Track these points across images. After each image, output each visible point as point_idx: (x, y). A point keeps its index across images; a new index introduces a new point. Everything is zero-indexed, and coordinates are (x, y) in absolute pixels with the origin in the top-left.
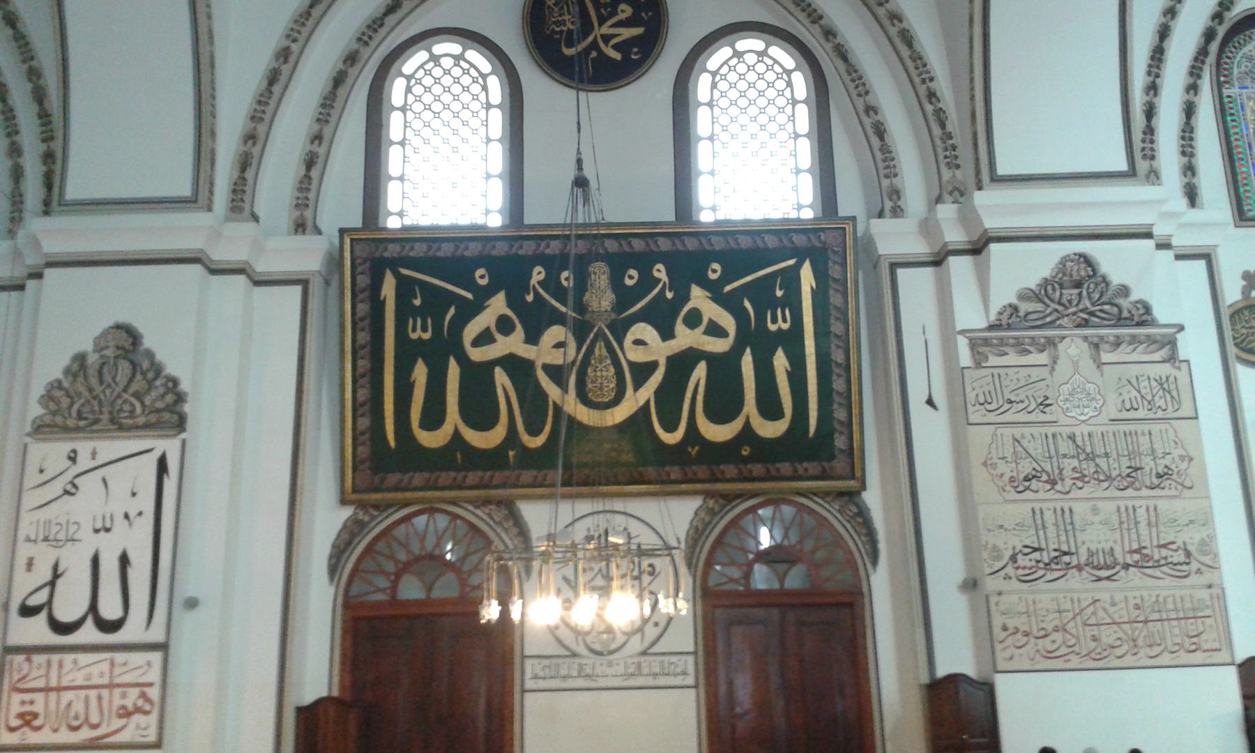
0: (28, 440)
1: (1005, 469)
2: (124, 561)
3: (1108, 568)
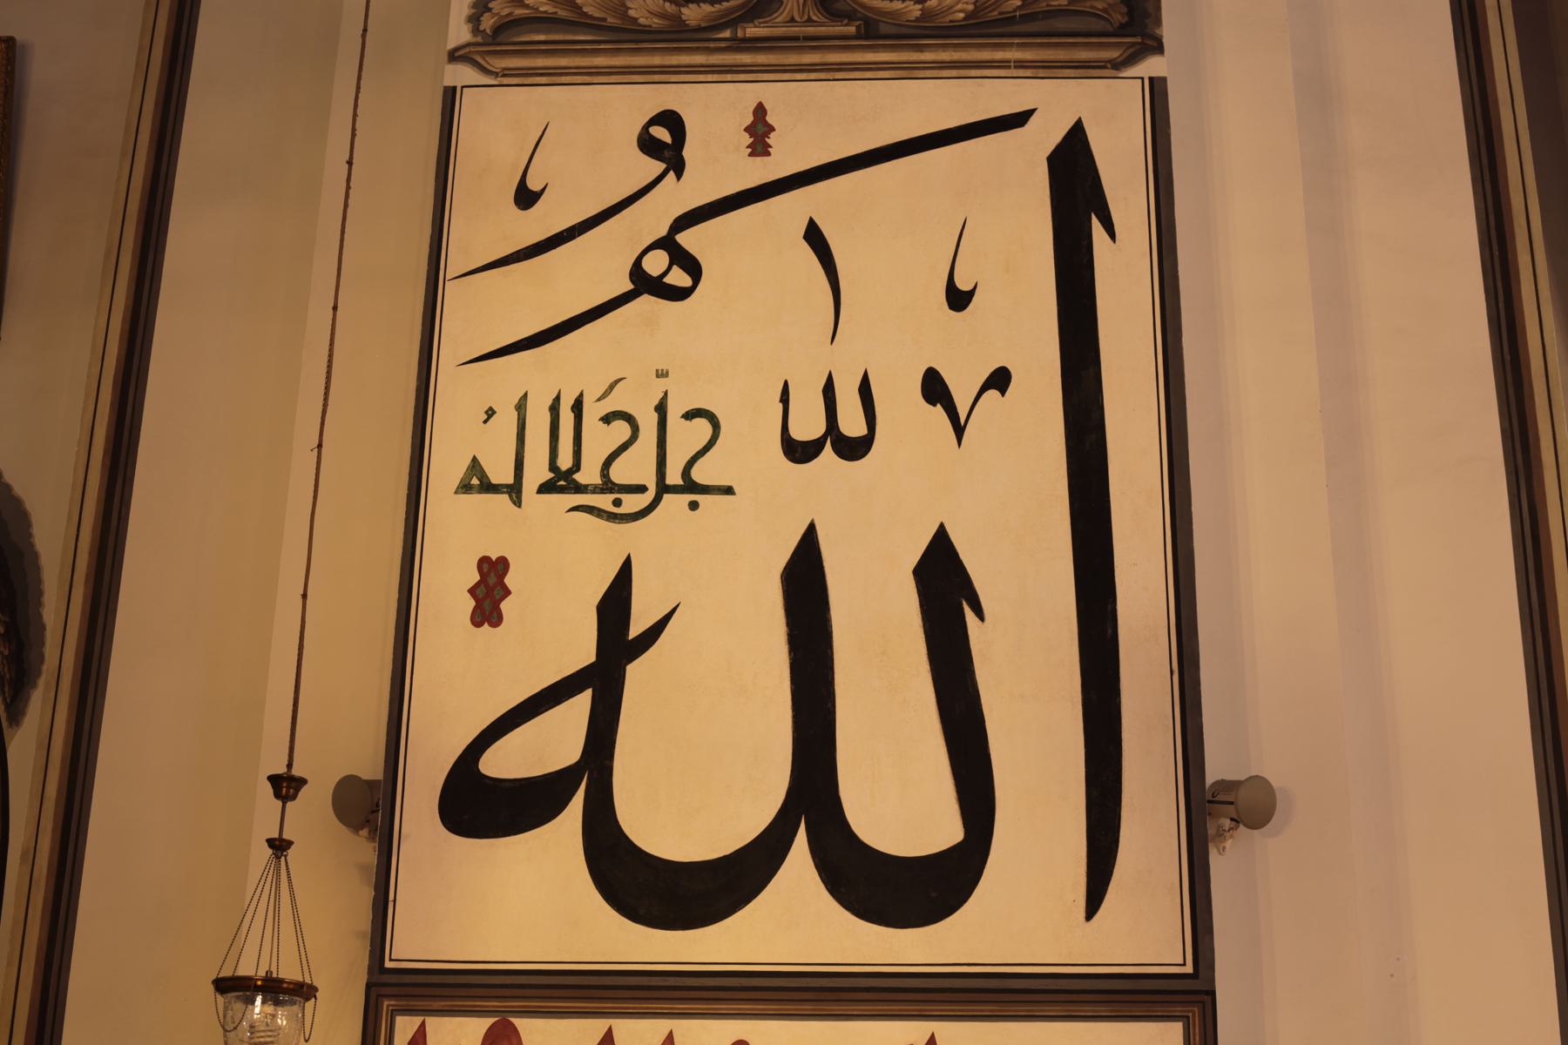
0: (461, 74)
2: (943, 583)
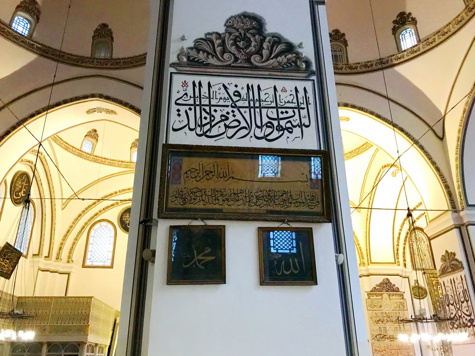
1: (374, 319)
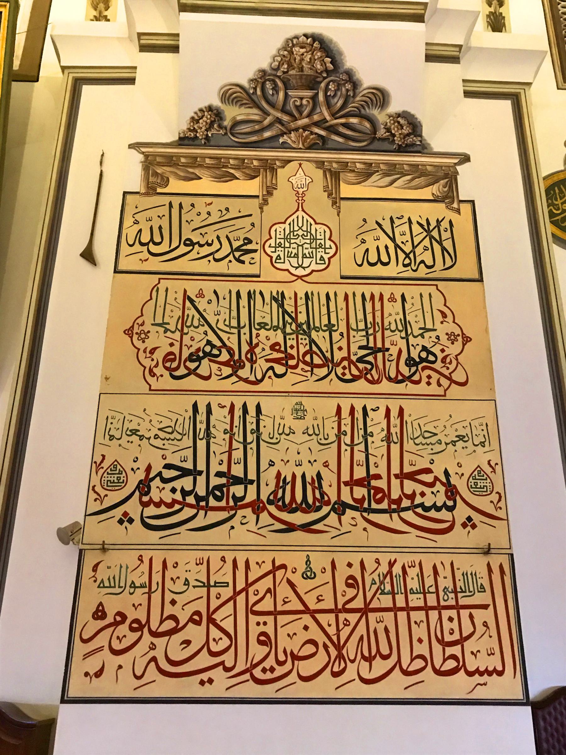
1: (161, 341)
3: (307, 508)
